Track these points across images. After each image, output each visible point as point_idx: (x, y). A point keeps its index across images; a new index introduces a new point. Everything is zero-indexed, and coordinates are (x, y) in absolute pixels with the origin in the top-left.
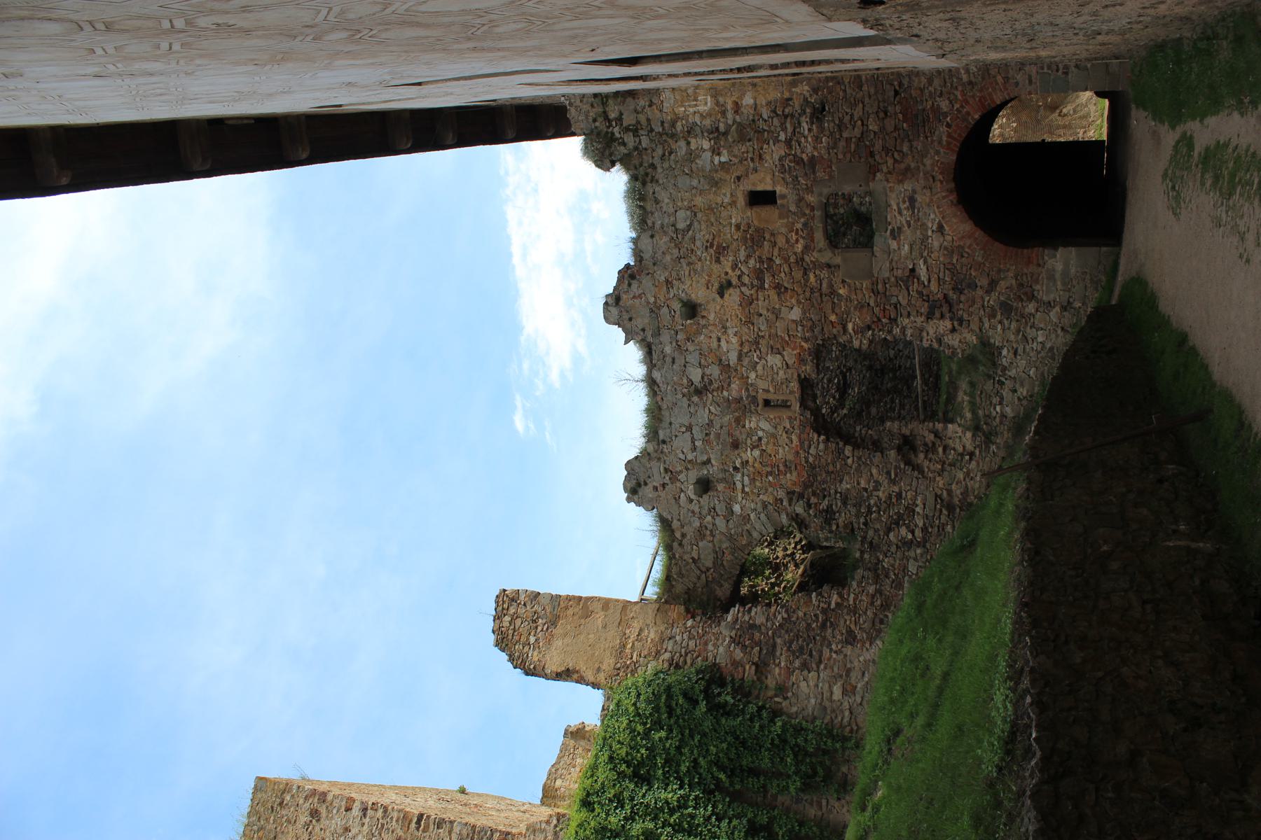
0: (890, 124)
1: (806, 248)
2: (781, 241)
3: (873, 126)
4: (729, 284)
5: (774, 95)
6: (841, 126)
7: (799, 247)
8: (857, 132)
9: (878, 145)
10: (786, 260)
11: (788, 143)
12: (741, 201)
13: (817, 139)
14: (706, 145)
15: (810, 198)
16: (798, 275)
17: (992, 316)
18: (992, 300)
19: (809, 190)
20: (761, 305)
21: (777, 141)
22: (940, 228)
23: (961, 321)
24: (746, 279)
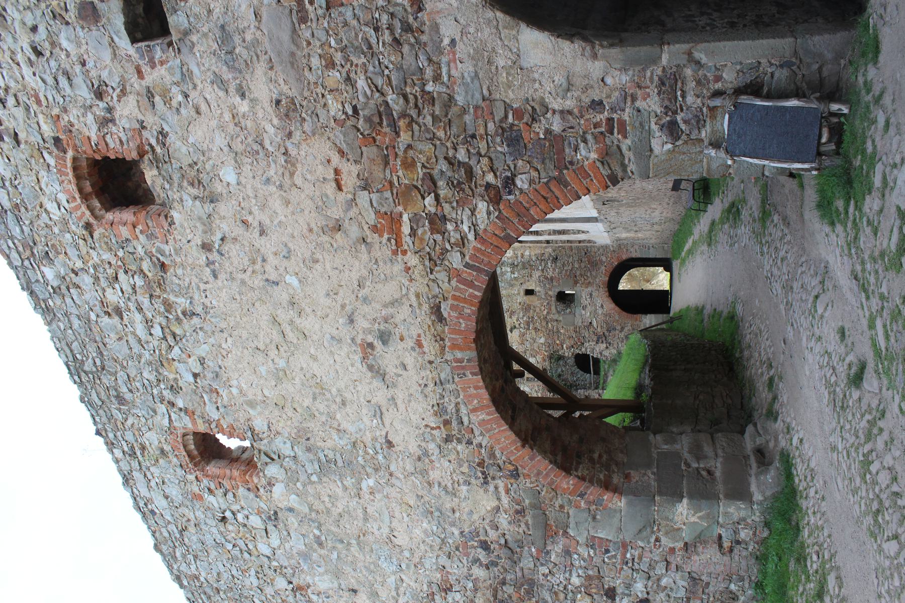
0: (583, 265)
1: (548, 313)
2: (538, 310)
3: (576, 266)
4: (515, 327)
5: (538, 252)
6: (564, 265)
7: (545, 312)
8: (570, 268)
9: (578, 273)
10: (539, 318)
11: (542, 270)
12: (522, 293)
13: (554, 270)
14: (509, 270)
15: (550, 293)
16: (544, 324)
17: (622, 342)
18: (622, 335)
19: (550, 289)
20: (528, 336)
21: (538, 269)
22: (602, 306)
23: (610, 344)
24: (522, 325)
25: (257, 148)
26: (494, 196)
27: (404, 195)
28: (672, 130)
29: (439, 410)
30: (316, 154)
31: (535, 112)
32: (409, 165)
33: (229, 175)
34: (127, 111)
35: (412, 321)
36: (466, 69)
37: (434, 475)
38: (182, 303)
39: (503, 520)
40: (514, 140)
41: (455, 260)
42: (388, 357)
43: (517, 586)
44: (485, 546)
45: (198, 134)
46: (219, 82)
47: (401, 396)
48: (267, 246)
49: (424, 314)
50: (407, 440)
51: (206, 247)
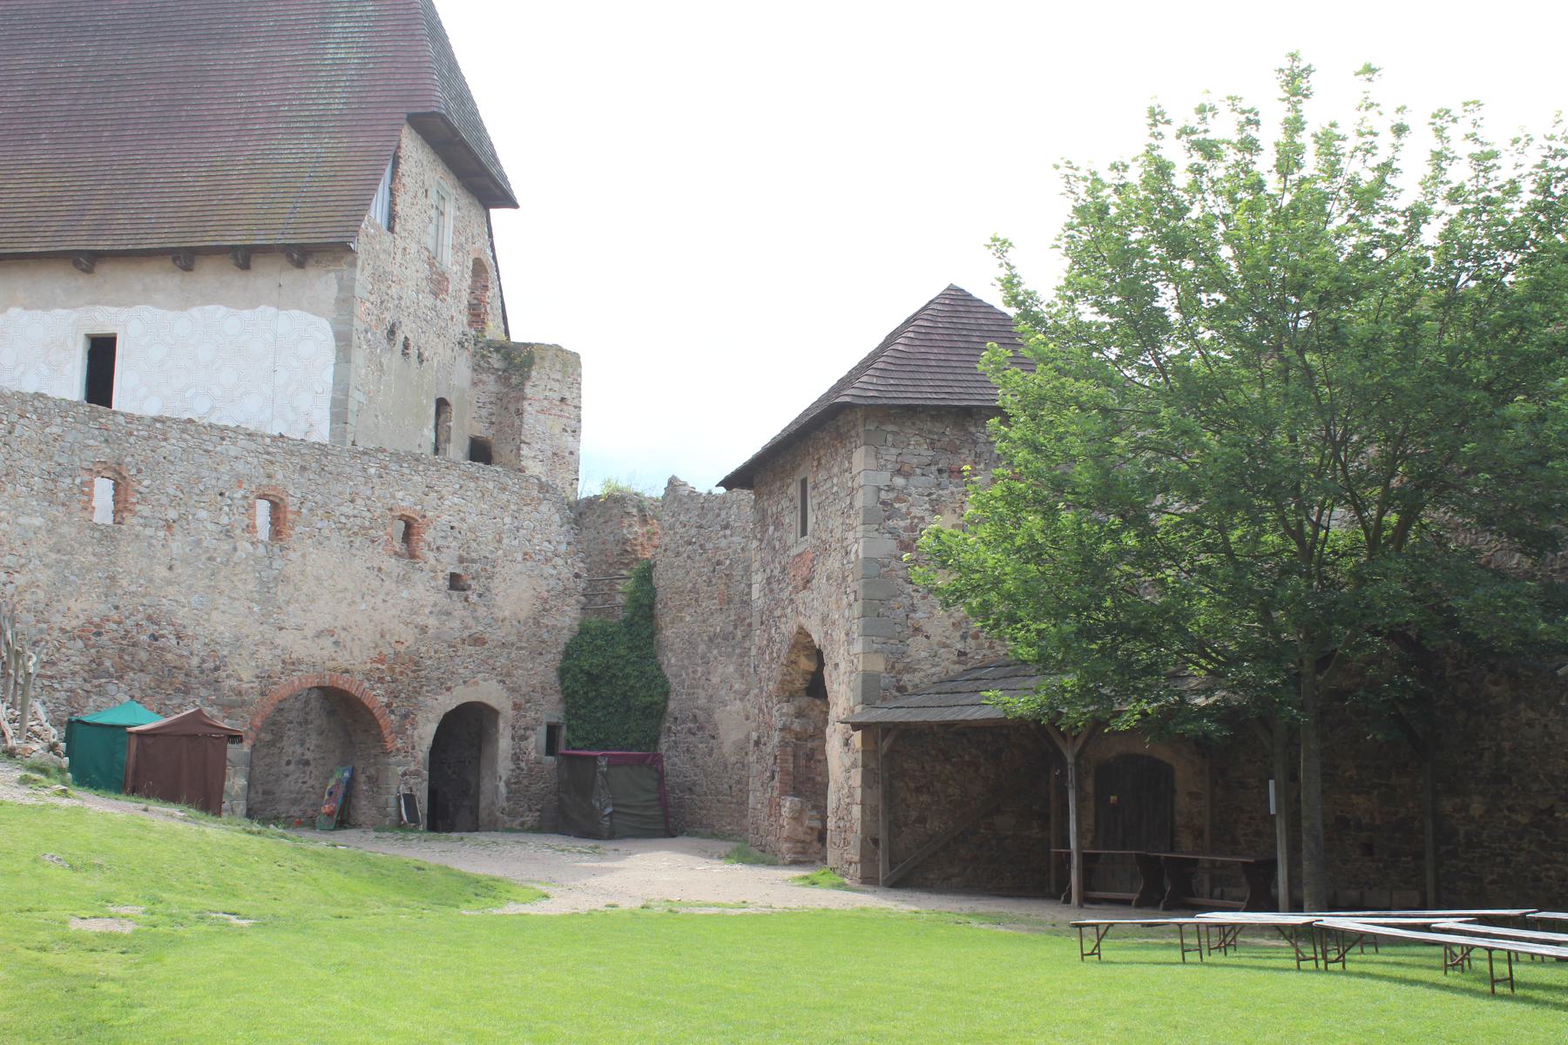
25: (414, 612)
26: (388, 705)
27: (392, 669)
28: (404, 774)
29: (300, 661)
30: (409, 636)
31: (414, 726)
32: (402, 673)
33: (405, 594)
34: (430, 556)
35: (343, 660)
36: (430, 702)
37: (262, 649)
38: (357, 544)
39: (233, 682)
40: (406, 716)
41: (366, 684)
42: (327, 642)
43: (184, 684)
44: (217, 669)
45: (420, 587)
46: (435, 605)
47: (309, 643)
48: (378, 600)
49: (345, 665)
50: (284, 639)
51: (380, 569)
